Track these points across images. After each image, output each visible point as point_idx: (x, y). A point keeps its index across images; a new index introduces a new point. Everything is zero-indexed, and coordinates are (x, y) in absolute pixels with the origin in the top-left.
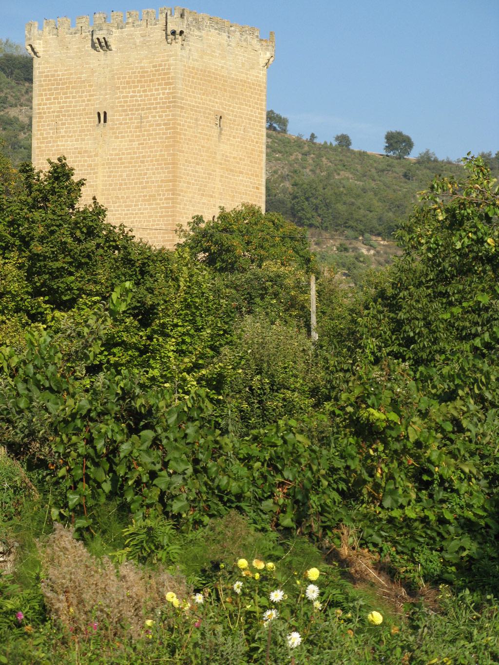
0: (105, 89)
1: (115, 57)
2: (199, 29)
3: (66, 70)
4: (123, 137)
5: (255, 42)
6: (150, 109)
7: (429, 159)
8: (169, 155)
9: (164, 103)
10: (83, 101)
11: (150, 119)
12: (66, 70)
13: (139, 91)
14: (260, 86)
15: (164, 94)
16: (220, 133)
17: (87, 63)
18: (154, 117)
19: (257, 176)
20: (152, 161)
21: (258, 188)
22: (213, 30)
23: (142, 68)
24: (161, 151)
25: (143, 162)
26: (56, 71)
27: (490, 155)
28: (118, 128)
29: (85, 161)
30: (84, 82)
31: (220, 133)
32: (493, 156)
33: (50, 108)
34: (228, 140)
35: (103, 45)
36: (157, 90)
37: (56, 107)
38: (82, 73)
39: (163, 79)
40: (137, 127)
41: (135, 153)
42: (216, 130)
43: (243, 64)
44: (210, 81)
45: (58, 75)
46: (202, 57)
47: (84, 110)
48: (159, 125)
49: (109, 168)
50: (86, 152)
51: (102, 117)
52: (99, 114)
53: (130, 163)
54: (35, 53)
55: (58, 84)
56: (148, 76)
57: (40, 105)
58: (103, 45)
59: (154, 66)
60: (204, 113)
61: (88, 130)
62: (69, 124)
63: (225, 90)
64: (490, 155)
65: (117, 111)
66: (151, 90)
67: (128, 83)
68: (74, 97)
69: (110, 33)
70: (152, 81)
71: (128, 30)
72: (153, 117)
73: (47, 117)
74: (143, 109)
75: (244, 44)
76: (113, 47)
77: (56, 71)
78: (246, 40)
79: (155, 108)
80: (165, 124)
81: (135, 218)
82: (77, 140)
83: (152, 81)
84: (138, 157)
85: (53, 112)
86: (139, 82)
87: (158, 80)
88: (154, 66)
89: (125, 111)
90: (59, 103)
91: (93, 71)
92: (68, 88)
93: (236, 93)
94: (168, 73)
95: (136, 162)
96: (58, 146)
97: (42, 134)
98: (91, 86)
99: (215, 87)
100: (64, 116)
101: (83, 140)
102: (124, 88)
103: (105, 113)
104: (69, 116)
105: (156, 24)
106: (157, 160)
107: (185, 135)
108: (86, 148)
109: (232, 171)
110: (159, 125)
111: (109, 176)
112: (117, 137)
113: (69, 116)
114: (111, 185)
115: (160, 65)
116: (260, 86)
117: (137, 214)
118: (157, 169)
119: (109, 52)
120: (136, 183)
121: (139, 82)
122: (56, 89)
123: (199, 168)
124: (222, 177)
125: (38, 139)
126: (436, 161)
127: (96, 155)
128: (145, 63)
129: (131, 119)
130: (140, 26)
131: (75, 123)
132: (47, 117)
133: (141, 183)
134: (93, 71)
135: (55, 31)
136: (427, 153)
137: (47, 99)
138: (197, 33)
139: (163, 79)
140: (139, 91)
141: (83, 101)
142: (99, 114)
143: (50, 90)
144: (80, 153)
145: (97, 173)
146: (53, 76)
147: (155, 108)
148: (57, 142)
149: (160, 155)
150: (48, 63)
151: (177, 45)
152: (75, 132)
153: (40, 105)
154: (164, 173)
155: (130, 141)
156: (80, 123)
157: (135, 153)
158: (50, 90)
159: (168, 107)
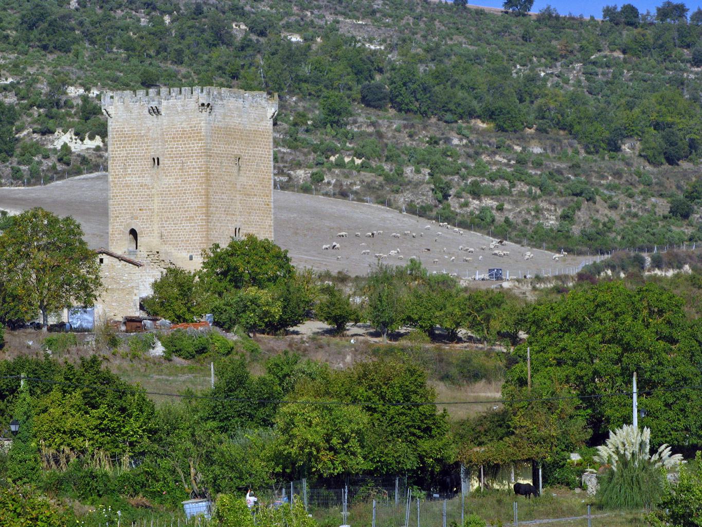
0: (158, 142)
1: (164, 119)
2: (221, 99)
4: (171, 176)
5: (263, 102)
6: (188, 157)
7: (550, 15)
8: (202, 189)
9: (198, 153)
10: (143, 150)
13: (181, 144)
14: (268, 132)
16: (239, 170)
17: (145, 123)
18: (192, 162)
19: (267, 196)
21: (268, 205)
22: (232, 99)
23: (182, 128)
25: (184, 193)
26: (124, 128)
27: (615, 8)
28: (167, 170)
29: (145, 192)
30: (143, 136)
31: (239, 170)
32: (619, 9)
34: (245, 173)
35: (155, 111)
36: (193, 144)
37: (124, 153)
38: (141, 130)
39: (197, 136)
40: (180, 169)
41: (179, 187)
42: (236, 168)
43: (255, 119)
44: (230, 135)
46: (224, 119)
48: (195, 168)
50: (145, 185)
51: (156, 161)
52: (154, 159)
53: (176, 194)
54: (109, 115)
55: (125, 137)
56: (187, 134)
57: (113, 151)
58: (155, 111)
59: (191, 127)
60: (227, 157)
61: (147, 170)
62: (134, 165)
63: (242, 139)
64: (615, 8)
65: (167, 158)
66: (189, 144)
67: (173, 138)
68: (136, 147)
69: (160, 103)
70: (189, 137)
71: (172, 101)
72: (191, 162)
73: (118, 160)
74: (184, 157)
75: (255, 104)
76: (163, 113)
77: (124, 128)
78: (256, 102)
79: (192, 156)
80: (199, 168)
82: (139, 177)
83: (189, 137)
84: (182, 190)
86: (181, 137)
87: (193, 137)
88: (191, 127)
89: (172, 157)
90: (126, 150)
91: (149, 129)
92: (132, 140)
93: (251, 140)
94: (201, 133)
95: (180, 193)
97: (115, 172)
98: (148, 139)
99: (235, 138)
100: (130, 159)
101: (143, 177)
102: (171, 141)
103: (158, 159)
104: (134, 159)
106: (194, 193)
107: (213, 174)
109: (248, 195)
110: (195, 168)
111: (162, 203)
112: (167, 176)
113: (134, 159)
114: (163, 209)
115: (195, 127)
116: (268, 132)
118: (194, 198)
121: (181, 137)
122: (124, 141)
123: (224, 196)
124: (241, 200)
126: (557, 18)
127: (153, 188)
128: (184, 125)
129: (176, 163)
130: (180, 98)
131: (138, 165)
132: (118, 160)
133: (184, 208)
134: (149, 129)
136: (548, 8)
137: (118, 148)
138: (220, 102)
139: (197, 136)
140: (181, 144)
141: (143, 150)
142: (154, 159)
143: (120, 141)
144: (141, 186)
146: (122, 131)
147: (192, 156)
149: (196, 189)
150: (118, 122)
151: (205, 114)
152: (138, 171)
153: (113, 151)
157: (179, 187)
158: (120, 141)
159: (201, 156)
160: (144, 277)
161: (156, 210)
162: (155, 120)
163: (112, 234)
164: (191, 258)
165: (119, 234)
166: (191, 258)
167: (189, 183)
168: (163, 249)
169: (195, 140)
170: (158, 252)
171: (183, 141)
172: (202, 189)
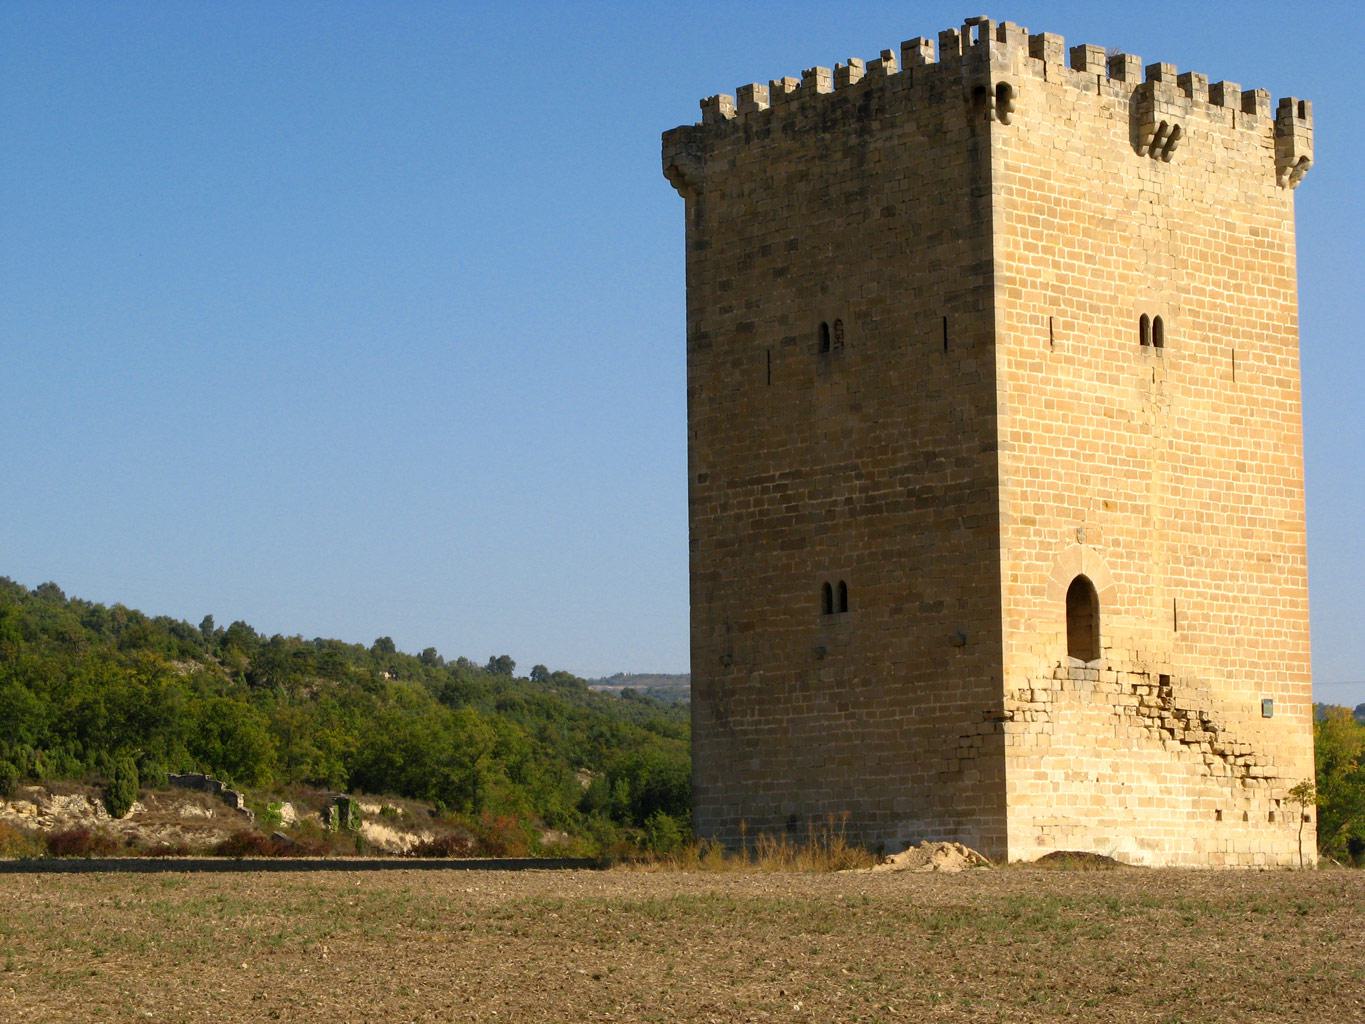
3: (1069, 180)
10: (1111, 276)
11: (1251, 362)
12: (1069, 180)
15: (1274, 305)
20: (1259, 469)
29: (1121, 439)
33: (1037, 274)
45: (1052, 189)
47: (1114, 299)
49: (1174, 469)
50: (1122, 413)
51: (1151, 332)
62: (1083, 329)
66: (1249, 290)
68: (1089, 259)
81: (1232, 609)
82: (1101, 378)
85: (1045, 286)
96: (1058, 383)
104: (1081, 306)
105: (1252, 128)
108: (1121, 403)
114: (1178, 514)
117: (1235, 599)
119: (1161, 164)
120: (1230, 520)
125: (1011, 352)
128: (1235, 216)
135: (1039, 63)
141: (1111, 276)
145: (1148, 476)
146: (1040, 186)
148: (1055, 371)
152: (1095, 353)
154: (1284, 504)
160: (1123, 774)
161: (1156, 516)
162: (1146, 172)
163: (1011, 590)
164: (1266, 708)
165: (1034, 591)
166: (1266, 708)
167: (1254, 433)
168: (1180, 668)
169: (1265, 281)
170: (1164, 680)
171: (1233, 275)
172: (1291, 459)
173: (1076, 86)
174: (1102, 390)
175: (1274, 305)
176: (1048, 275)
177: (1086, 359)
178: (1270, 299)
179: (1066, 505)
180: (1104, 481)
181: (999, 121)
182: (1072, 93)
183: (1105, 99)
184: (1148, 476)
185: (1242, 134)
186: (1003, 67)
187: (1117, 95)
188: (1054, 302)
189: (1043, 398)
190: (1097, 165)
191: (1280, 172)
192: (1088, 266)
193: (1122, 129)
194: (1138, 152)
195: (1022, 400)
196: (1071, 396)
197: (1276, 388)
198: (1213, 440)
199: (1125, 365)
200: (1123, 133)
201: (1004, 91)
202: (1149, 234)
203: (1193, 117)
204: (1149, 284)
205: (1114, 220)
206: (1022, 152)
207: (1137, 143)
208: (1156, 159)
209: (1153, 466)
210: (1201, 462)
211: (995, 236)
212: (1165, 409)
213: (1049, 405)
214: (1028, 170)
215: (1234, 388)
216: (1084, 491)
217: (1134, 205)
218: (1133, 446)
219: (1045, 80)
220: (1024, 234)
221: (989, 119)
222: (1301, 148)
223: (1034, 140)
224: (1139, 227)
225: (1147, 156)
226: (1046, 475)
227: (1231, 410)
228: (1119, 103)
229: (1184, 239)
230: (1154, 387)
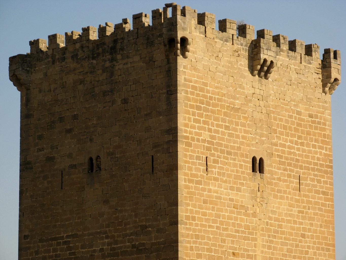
3: (217, 88)
10: (238, 136)
11: (309, 182)
12: (217, 88)
15: (321, 153)
20: (312, 237)
24: (321, 226)
29: (242, 220)
33: (200, 134)
45: (208, 92)
47: (239, 148)
49: (269, 236)
50: (242, 207)
51: (258, 166)
62: (223, 163)
66: (308, 145)
68: (227, 128)
73: (197, 146)
82: (232, 188)
85: (204, 141)
90: (210, 130)
96: (210, 191)
104: (222, 152)
105: (310, 63)
119: (264, 80)
125: (186, 174)
128: (301, 108)
135: (202, 28)
146: (202, 90)
148: (209, 184)
152: (229, 176)
155: (291, 205)
156: (235, 165)
162: (257, 85)
167: (311, 219)
169: (316, 141)
171: (300, 137)
173: (221, 40)
174: (233, 195)
175: (321, 153)
176: (206, 135)
177: (224, 179)
178: (318, 150)
179: (213, 254)
180: (233, 242)
181: (181, 56)
182: (219, 43)
183: (236, 47)
184: (255, 239)
185: (305, 66)
186: (184, 29)
187: (242, 45)
188: (208, 149)
189: (202, 198)
190: (231, 80)
191: (324, 86)
192: (226, 131)
193: (244, 62)
194: (252, 73)
195: (191, 199)
196: (217, 197)
197: (321, 195)
198: (289, 221)
199: (245, 182)
200: (245, 64)
201: (184, 41)
202: (257, 116)
203: (281, 57)
204: (257, 141)
205: (240, 108)
206: (193, 72)
207: (252, 69)
208: (261, 77)
209: (258, 234)
210: (283, 233)
211: (178, 115)
212: (264, 205)
213: (205, 202)
214: (196, 82)
215: (299, 195)
216: (222, 247)
217: (250, 101)
218: (248, 224)
219: (206, 36)
220: (194, 114)
221: (176, 55)
222: (334, 74)
223: (200, 66)
224: (252, 112)
225: (257, 76)
226: (203, 238)
227: (298, 206)
228: (243, 49)
229: (275, 119)
230: (259, 194)
